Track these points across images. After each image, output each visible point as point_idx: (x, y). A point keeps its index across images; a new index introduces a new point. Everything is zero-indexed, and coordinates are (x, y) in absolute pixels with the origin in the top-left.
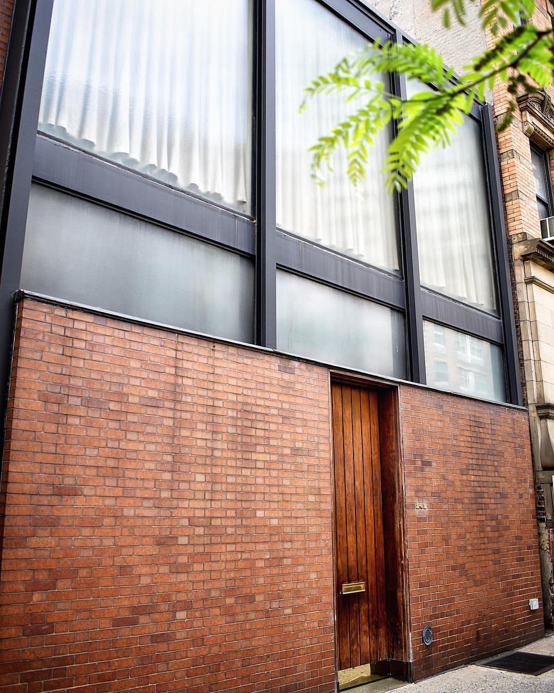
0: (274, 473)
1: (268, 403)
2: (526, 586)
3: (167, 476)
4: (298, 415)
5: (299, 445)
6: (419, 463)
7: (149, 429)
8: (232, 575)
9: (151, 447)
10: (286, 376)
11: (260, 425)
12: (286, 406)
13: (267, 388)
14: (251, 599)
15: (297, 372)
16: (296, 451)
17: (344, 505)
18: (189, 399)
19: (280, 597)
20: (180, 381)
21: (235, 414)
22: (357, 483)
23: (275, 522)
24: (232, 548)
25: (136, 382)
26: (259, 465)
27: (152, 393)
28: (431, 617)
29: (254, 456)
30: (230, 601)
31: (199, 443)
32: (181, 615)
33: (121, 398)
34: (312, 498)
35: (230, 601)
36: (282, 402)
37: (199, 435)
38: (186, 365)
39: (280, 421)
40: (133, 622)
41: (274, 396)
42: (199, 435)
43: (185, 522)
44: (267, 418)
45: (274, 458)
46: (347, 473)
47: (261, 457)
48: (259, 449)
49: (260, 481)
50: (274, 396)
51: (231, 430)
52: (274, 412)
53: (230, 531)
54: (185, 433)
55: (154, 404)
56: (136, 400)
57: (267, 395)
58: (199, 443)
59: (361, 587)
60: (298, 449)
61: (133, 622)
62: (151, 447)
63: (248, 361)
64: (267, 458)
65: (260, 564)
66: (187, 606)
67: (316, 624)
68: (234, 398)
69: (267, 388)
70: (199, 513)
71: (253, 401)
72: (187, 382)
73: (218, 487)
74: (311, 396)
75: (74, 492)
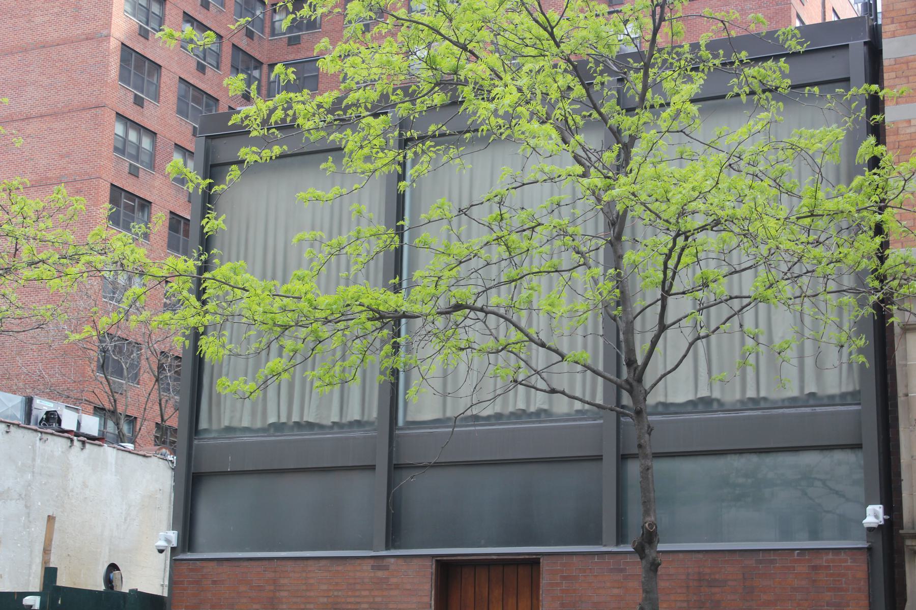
1: (359, 600)
10: (380, 574)
12: (378, 599)
13: (358, 587)
15: (392, 567)
20: (277, 594)
25: (244, 600)
36: (374, 596)
38: (282, 581)
41: (364, 593)
57: (357, 593)
63: (340, 568)
68: (325, 600)
69: (358, 587)
71: (343, 600)
74: (409, 587)
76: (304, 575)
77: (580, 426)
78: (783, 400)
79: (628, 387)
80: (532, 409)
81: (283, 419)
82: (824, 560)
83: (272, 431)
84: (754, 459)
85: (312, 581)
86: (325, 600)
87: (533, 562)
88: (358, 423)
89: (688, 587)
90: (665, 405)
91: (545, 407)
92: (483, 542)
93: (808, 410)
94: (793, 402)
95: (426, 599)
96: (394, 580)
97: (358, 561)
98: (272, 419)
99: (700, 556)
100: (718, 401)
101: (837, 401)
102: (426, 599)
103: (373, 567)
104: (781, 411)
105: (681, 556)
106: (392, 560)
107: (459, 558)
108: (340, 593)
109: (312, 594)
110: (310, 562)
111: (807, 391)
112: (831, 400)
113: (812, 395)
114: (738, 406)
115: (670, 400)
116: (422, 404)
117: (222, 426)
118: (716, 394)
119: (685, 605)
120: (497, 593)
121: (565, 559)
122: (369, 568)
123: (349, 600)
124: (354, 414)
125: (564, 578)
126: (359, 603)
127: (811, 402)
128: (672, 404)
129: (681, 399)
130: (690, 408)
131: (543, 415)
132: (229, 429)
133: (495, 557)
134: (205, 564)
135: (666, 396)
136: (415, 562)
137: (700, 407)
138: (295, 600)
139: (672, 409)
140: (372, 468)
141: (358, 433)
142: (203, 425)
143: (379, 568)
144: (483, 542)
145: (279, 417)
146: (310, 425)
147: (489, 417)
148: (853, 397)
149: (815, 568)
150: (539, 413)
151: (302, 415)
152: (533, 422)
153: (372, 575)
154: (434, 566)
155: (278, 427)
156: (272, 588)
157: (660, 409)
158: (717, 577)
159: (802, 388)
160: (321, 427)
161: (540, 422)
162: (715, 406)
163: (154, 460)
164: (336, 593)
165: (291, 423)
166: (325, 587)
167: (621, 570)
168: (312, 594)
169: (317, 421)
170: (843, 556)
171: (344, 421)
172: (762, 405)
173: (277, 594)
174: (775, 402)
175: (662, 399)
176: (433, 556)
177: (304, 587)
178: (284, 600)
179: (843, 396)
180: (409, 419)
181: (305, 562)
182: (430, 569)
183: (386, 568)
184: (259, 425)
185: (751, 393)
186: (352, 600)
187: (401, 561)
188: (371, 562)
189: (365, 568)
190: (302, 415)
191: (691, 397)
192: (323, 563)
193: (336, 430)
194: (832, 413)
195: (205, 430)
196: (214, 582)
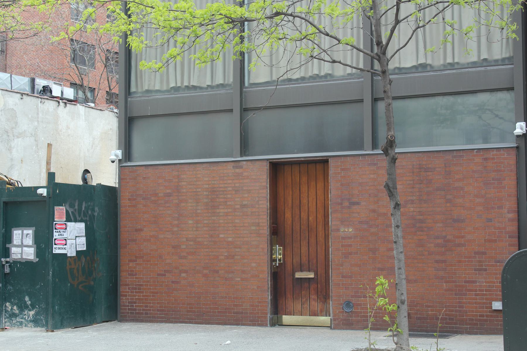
0: (230, 217)
1: (226, 185)
2: (480, 290)
3: (176, 222)
4: (244, 188)
5: (244, 203)
6: (346, 204)
7: (167, 205)
8: (207, 261)
9: (169, 212)
10: (238, 171)
11: (222, 196)
12: (237, 185)
13: (225, 178)
14: (217, 272)
16: (243, 206)
17: (299, 231)
18: (184, 191)
19: (233, 272)
20: (180, 184)
21: (207, 193)
22: (310, 218)
23: (230, 239)
24: (207, 250)
26: (221, 214)
27: (168, 191)
28: (352, 296)
29: (218, 211)
30: (205, 271)
31: (190, 208)
32: (183, 275)
33: (156, 195)
34: (253, 228)
35: (205, 271)
37: (190, 205)
38: (182, 176)
39: (234, 192)
40: (165, 275)
42: (190, 205)
43: (185, 240)
44: (225, 193)
45: (229, 210)
46: (302, 214)
47: (222, 211)
48: (220, 207)
49: (221, 221)
50: (230, 181)
51: (205, 200)
52: (230, 189)
53: (205, 243)
54: (183, 204)
55: (169, 195)
56: (162, 195)
57: (225, 182)
58: (190, 208)
59: (311, 275)
60: (245, 205)
61: (165, 275)
62: (169, 212)
63: (215, 168)
64: (226, 211)
65: (223, 257)
66: (186, 272)
67: (255, 287)
68: (207, 186)
69: (225, 178)
70: (190, 236)
72: (183, 183)
73: (199, 225)
74: (254, 177)
75: (141, 230)
76: (195, 172)
77: (350, 83)
78: (468, 64)
79: (377, 57)
80: (322, 74)
81: (179, 85)
82: (491, 155)
83: (173, 91)
84: (451, 99)
85: (199, 176)
86: (207, 186)
87: (325, 162)
88: (222, 85)
89: (413, 172)
90: (399, 69)
91: (330, 72)
92: (296, 151)
93: (483, 69)
94: (474, 64)
95: (264, 184)
96: (245, 174)
97: (225, 164)
98: (172, 85)
99: (420, 154)
100: (430, 65)
101: (500, 63)
102: (264, 184)
103: (234, 167)
104: (467, 70)
105: (409, 154)
106: (245, 163)
107: (282, 160)
108: (215, 182)
109: (200, 183)
110: (198, 165)
111: (482, 58)
112: (496, 62)
113: (485, 60)
114: (442, 68)
115: (402, 66)
116: (259, 73)
117: (144, 90)
118: (429, 62)
119: (412, 182)
120: (304, 179)
121: (343, 159)
122: (232, 167)
123: (221, 186)
124: (219, 80)
125: (342, 170)
126: (226, 187)
127: (485, 64)
128: (403, 68)
129: (408, 65)
130: (414, 70)
131: (329, 78)
132: (148, 91)
133: (303, 159)
134: (138, 168)
135: (400, 63)
136: (258, 163)
137: (420, 69)
138: (190, 187)
139: (404, 71)
140: (231, 111)
141: (222, 91)
142: (133, 89)
143: (237, 167)
144: (296, 151)
145: (176, 84)
146: (195, 87)
147: (297, 80)
148: (509, 60)
149: (486, 159)
150: (326, 76)
151: (189, 82)
152: (323, 81)
153: (233, 171)
154: (268, 165)
155: (176, 89)
156: (177, 180)
157: (397, 71)
158: (430, 166)
159: (479, 56)
160: (201, 88)
161: (327, 81)
162: (429, 68)
163: (107, 112)
164: (213, 182)
165: (183, 87)
166: (207, 179)
167: (375, 164)
168: (200, 183)
169: (198, 85)
170: (502, 152)
171: (214, 84)
172: (456, 67)
173: (180, 184)
174: (463, 65)
175: (398, 66)
176: (267, 160)
177: (195, 179)
178: (184, 187)
179: (503, 60)
180: (251, 82)
181: (195, 165)
182: (266, 167)
183: (241, 167)
184: (165, 88)
185: (449, 60)
186: (223, 186)
187: (249, 163)
188: (233, 164)
189: (229, 167)
190: (189, 82)
191: (414, 64)
192: (205, 165)
193: (209, 89)
194: (497, 70)
195: (134, 92)
196: (144, 178)
